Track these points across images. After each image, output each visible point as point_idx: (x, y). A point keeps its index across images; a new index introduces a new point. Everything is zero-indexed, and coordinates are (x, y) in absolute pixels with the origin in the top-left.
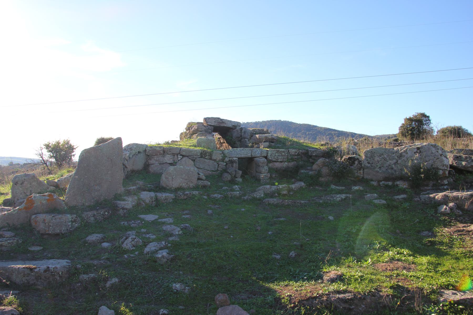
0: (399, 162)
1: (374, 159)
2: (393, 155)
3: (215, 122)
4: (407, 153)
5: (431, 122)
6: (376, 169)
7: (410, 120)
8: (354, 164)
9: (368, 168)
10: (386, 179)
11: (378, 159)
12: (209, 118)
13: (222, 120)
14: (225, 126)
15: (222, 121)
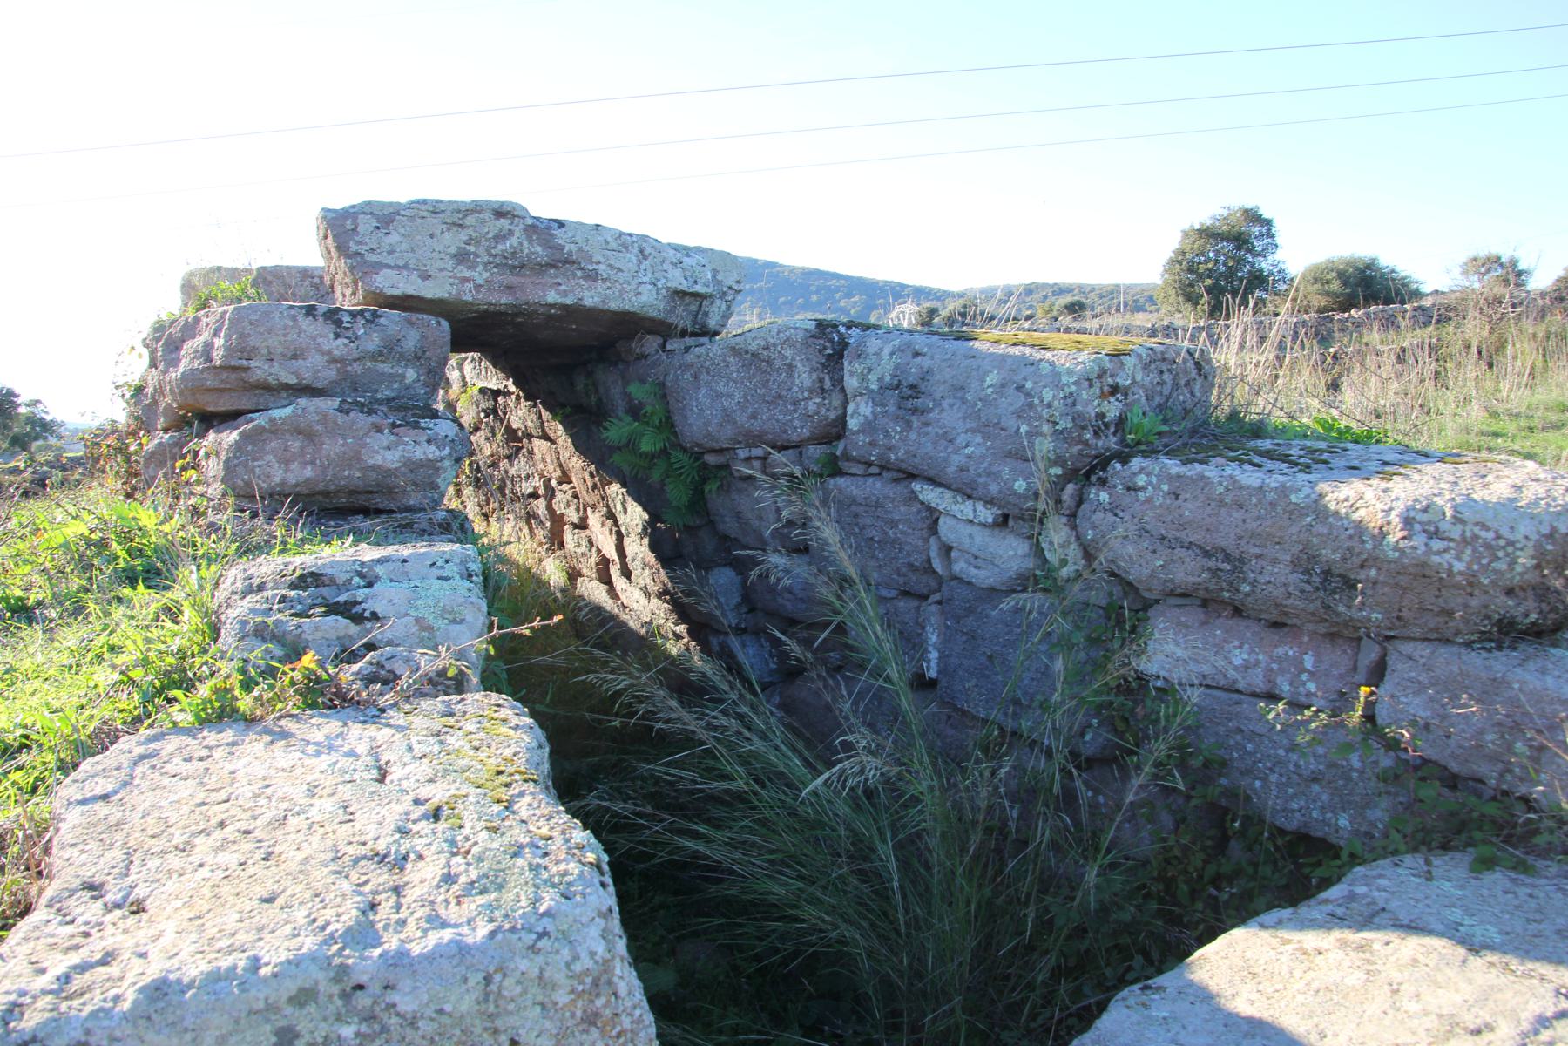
3: (462, 257)
5: (1278, 240)
7: (1208, 234)
12: (386, 216)
13: (543, 230)
14: (591, 297)
15: (551, 244)
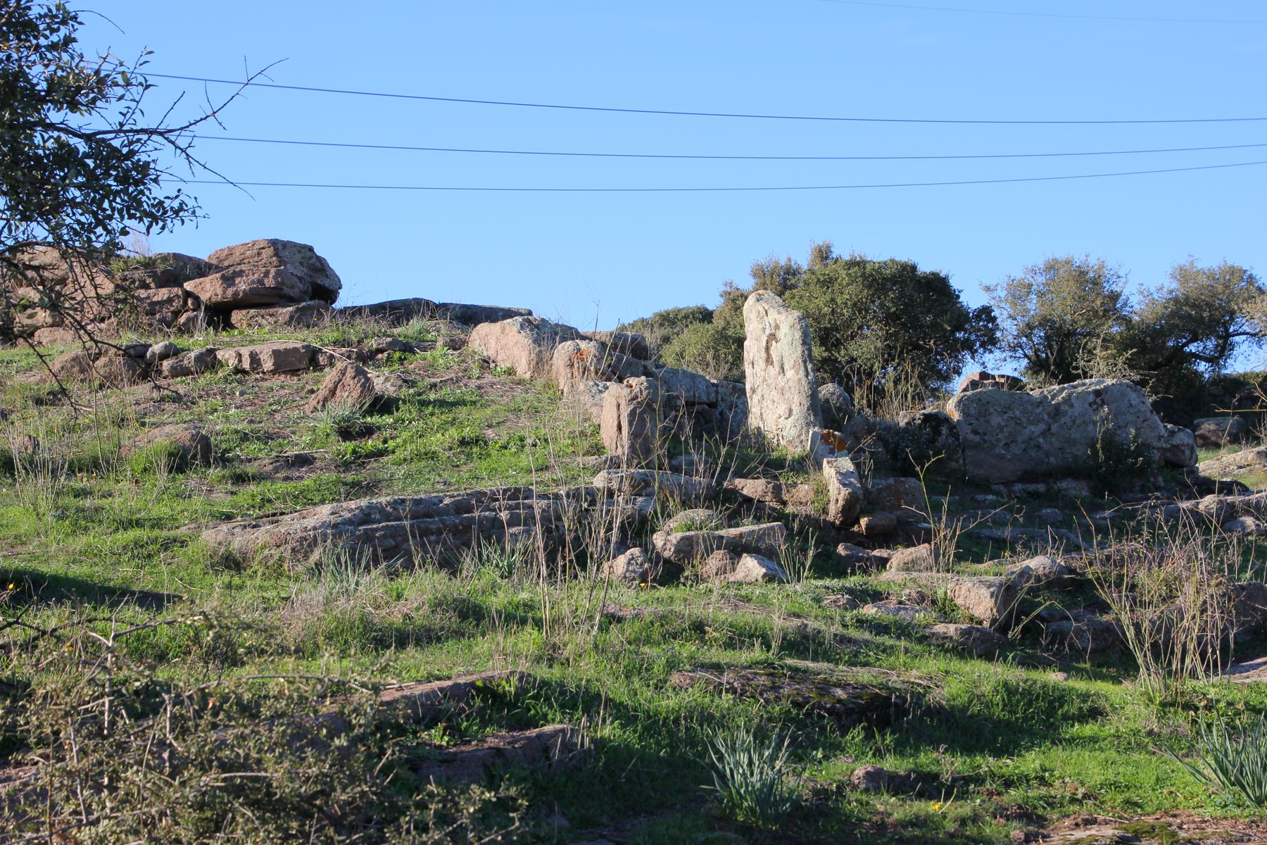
0: (1054, 428)
1: (988, 421)
2: (1037, 411)
4: (1072, 406)
6: (997, 451)
8: (940, 434)
9: (975, 446)
10: (1028, 476)
11: (999, 420)
12: (285, 245)
